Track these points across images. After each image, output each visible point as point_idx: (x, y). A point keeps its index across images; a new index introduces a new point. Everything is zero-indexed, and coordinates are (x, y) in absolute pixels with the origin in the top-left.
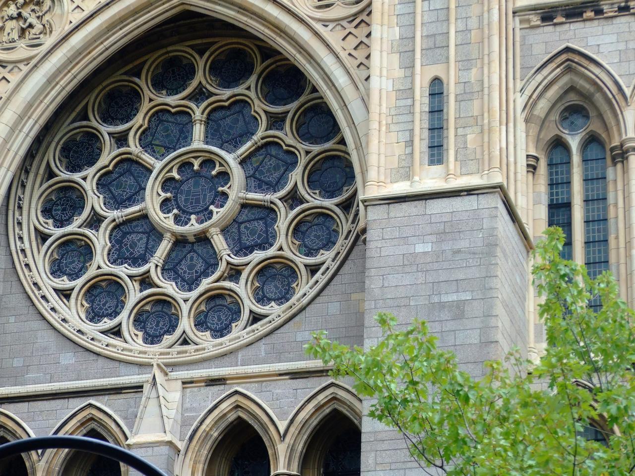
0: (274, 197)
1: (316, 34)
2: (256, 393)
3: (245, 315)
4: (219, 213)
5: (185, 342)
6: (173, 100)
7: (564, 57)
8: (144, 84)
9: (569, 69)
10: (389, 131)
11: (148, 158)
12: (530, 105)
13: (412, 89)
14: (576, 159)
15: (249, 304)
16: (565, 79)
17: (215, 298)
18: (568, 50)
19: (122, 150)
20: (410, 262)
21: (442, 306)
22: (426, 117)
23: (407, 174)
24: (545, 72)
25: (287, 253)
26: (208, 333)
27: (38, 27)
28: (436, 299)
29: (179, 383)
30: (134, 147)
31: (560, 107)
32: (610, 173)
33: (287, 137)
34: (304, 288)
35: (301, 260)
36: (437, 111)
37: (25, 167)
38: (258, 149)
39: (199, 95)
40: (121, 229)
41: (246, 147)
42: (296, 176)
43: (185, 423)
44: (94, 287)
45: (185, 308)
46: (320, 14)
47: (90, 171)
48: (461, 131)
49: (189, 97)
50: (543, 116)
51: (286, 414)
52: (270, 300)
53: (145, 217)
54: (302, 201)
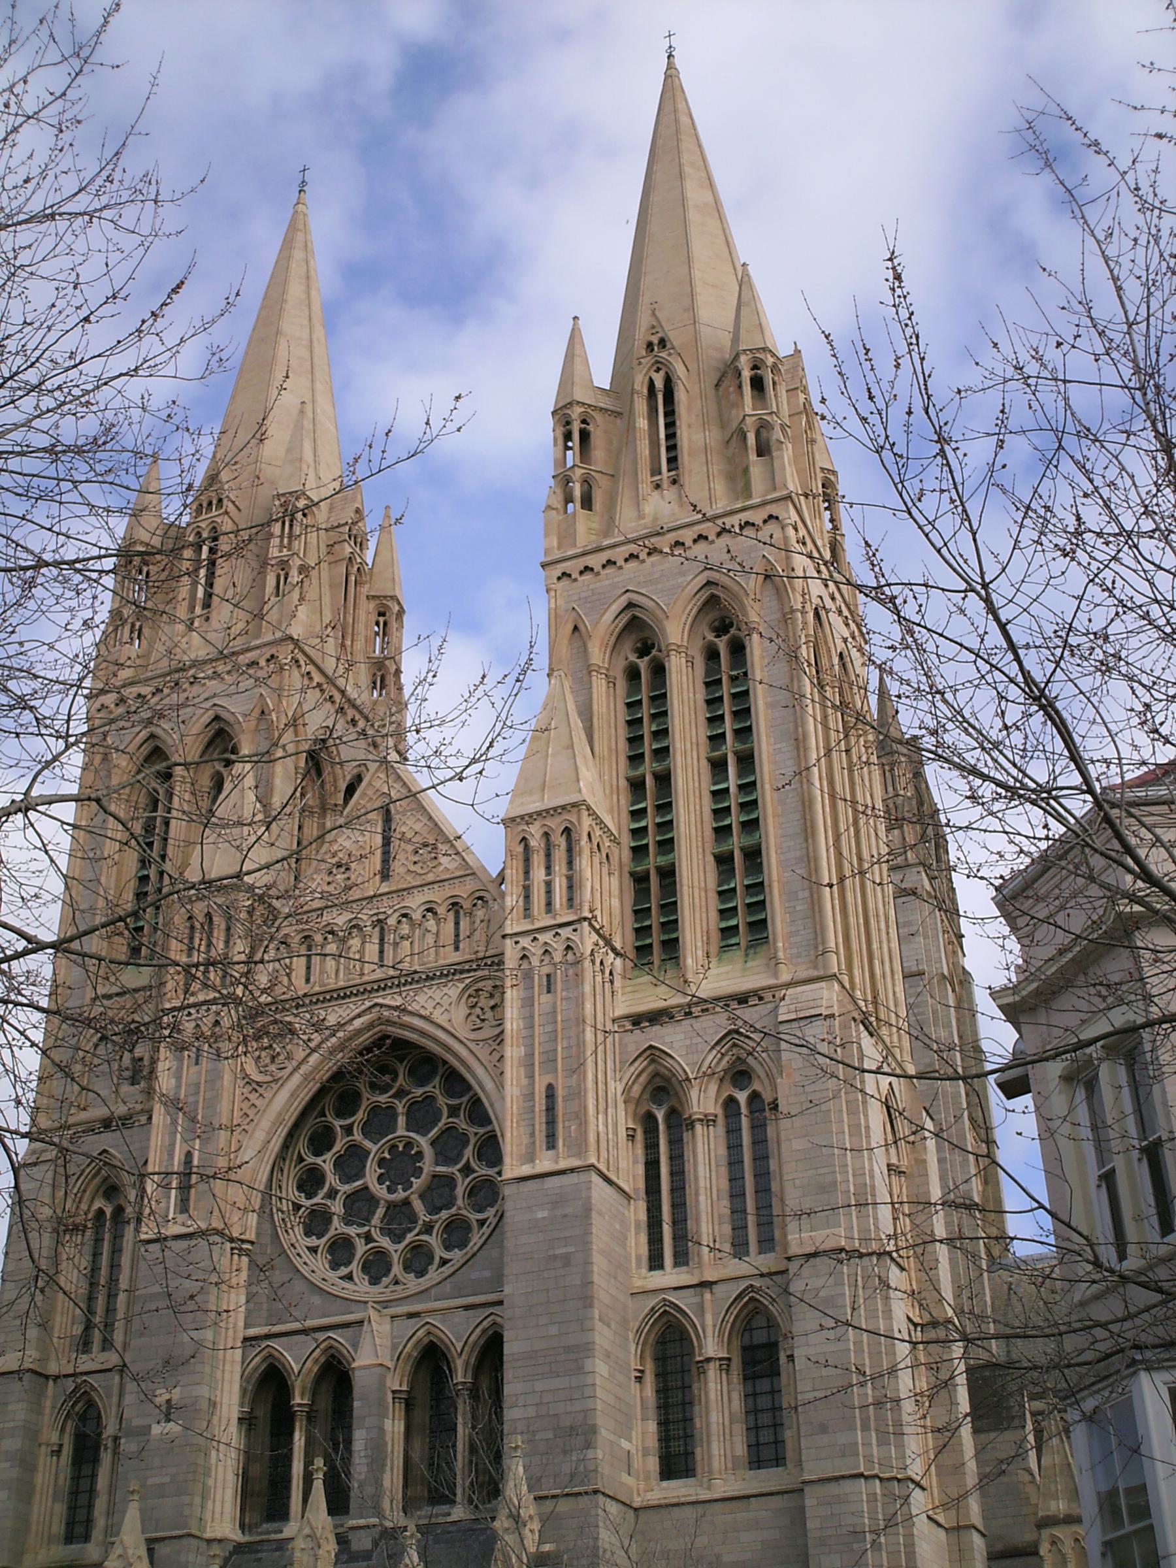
0: (454, 1170)
1: (472, 1052)
2: (442, 1322)
3: (437, 1260)
4: (417, 1183)
5: (397, 1283)
6: (383, 1099)
7: (648, 1052)
8: (362, 1086)
9: (653, 1061)
10: (518, 1126)
11: (367, 1144)
12: (627, 1090)
13: (533, 1093)
14: (662, 1127)
15: (439, 1252)
16: (651, 1068)
18: (651, 1047)
19: (350, 1138)
21: (555, 1257)
22: (544, 1114)
23: (531, 1158)
24: (636, 1064)
26: (412, 1275)
28: (551, 1253)
29: (389, 1318)
30: (357, 1136)
31: (650, 1088)
32: (685, 1135)
33: (462, 1123)
34: (476, 1239)
35: (474, 1217)
36: (550, 1109)
37: (281, 1156)
38: (443, 1132)
39: (401, 1094)
40: (350, 1198)
41: (434, 1132)
42: (468, 1152)
43: (394, 1347)
44: (333, 1243)
45: (395, 1257)
46: (473, 1036)
47: (328, 1156)
48: (567, 1124)
49: (394, 1096)
50: (637, 1096)
51: (462, 1337)
52: (454, 1247)
53: (367, 1188)
54: (474, 1171)
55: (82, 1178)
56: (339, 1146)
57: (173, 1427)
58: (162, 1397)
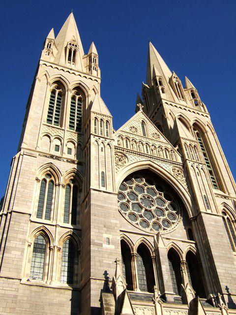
17: (155, 223)
20: (211, 225)
21: (219, 235)
25: (168, 218)
27: (123, 161)
42: (167, 205)
55: (42, 167)
56: (129, 190)
57: (112, 247)
58: (105, 236)
